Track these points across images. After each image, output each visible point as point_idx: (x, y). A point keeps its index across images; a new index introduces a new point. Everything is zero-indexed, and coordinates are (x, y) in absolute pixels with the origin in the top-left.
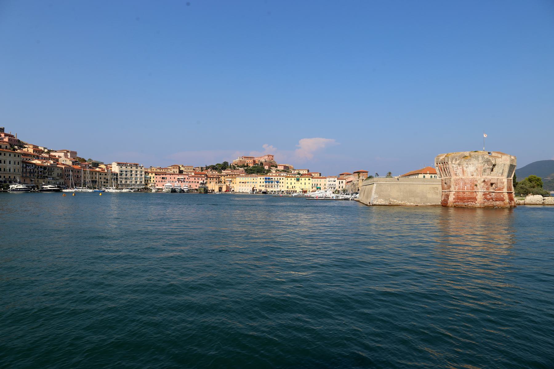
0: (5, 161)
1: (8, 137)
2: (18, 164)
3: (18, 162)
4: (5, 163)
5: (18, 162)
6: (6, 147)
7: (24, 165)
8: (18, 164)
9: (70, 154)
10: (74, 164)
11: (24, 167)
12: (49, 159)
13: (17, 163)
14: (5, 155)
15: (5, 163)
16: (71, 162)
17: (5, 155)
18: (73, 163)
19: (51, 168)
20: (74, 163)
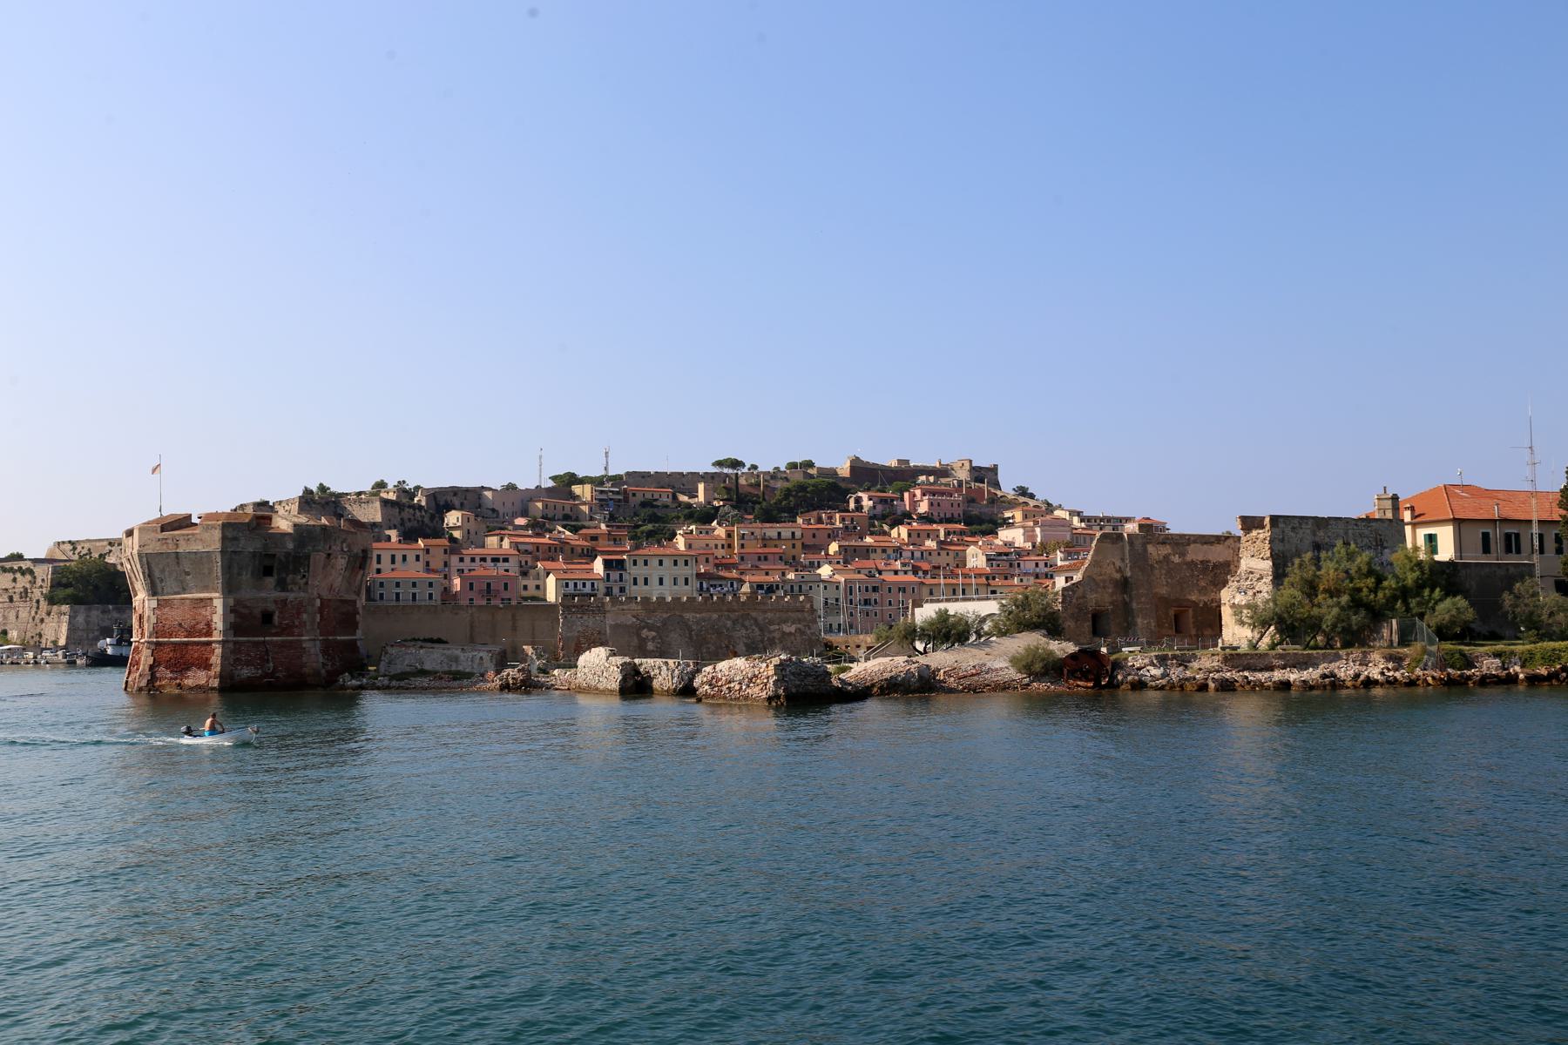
0: (646, 580)
1: (927, 497)
2: (686, 583)
3: (686, 580)
4: (646, 583)
5: (686, 580)
6: (793, 533)
7: (705, 585)
8: (686, 583)
9: (1042, 531)
10: (994, 562)
11: (705, 589)
12: (939, 554)
13: (681, 581)
14: (646, 563)
15: (646, 583)
16: (984, 558)
17: (646, 563)
18: (988, 560)
19: (800, 587)
20: (994, 560)
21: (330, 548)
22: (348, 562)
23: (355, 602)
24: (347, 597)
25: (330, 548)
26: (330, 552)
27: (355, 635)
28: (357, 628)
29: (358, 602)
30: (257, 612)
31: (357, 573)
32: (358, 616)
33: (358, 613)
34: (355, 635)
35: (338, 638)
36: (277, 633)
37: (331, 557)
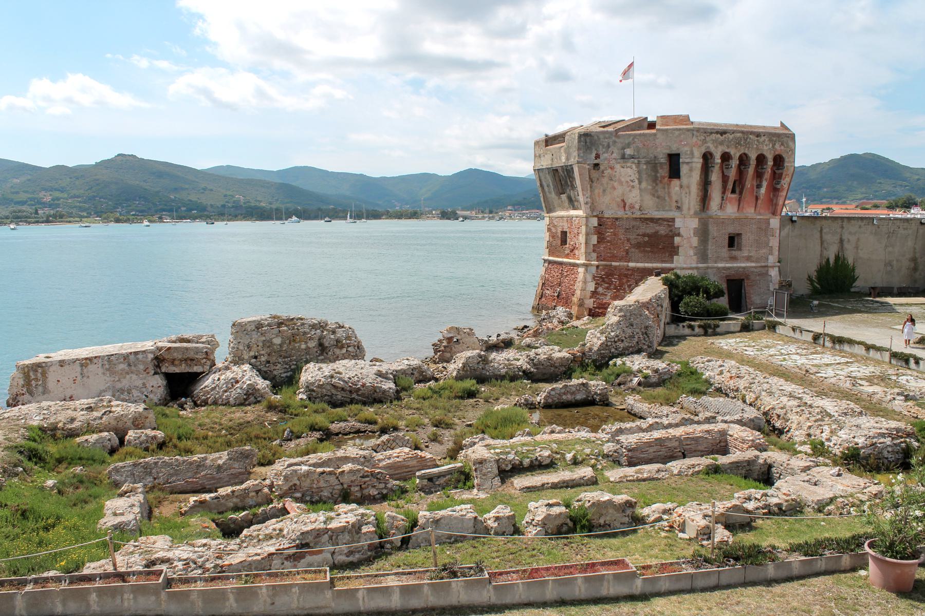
21: (597, 157)
22: (639, 172)
23: (673, 220)
24: (657, 215)
25: (597, 157)
26: (596, 162)
27: (672, 262)
28: (677, 254)
29: (677, 220)
30: (559, 230)
31: (669, 185)
32: (677, 240)
33: (679, 235)
34: (672, 262)
35: (632, 265)
36: (568, 254)
37: (602, 167)
